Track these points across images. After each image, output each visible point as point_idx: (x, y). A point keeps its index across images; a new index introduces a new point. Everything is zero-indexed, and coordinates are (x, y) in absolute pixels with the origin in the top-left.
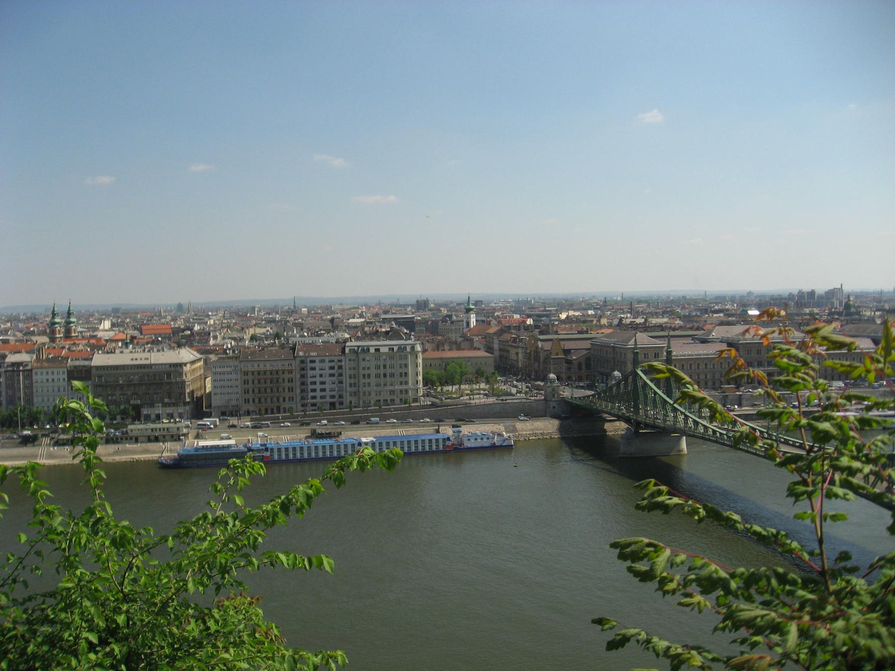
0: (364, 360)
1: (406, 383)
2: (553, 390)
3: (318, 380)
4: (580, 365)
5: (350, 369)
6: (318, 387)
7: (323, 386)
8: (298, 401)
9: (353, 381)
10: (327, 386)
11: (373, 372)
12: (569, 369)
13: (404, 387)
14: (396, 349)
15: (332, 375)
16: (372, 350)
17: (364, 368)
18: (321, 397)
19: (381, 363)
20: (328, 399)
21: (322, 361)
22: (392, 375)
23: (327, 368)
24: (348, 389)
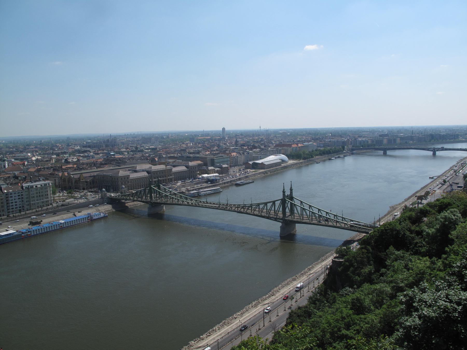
0: (31, 191)
1: (48, 198)
2: (105, 194)
3: (14, 201)
4: (90, 183)
5: (26, 195)
6: (14, 204)
7: (16, 204)
8: (6, 211)
9: (27, 200)
10: (18, 203)
11: (35, 195)
12: (87, 185)
13: (47, 200)
14: (43, 185)
15: (19, 199)
16: (34, 187)
17: (32, 194)
18: (16, 208)
19: (38, 191)
20: (18, 209)
21: (15, 193)
22: (42, 196)
23: (17, 196)
24: (26, 203)
